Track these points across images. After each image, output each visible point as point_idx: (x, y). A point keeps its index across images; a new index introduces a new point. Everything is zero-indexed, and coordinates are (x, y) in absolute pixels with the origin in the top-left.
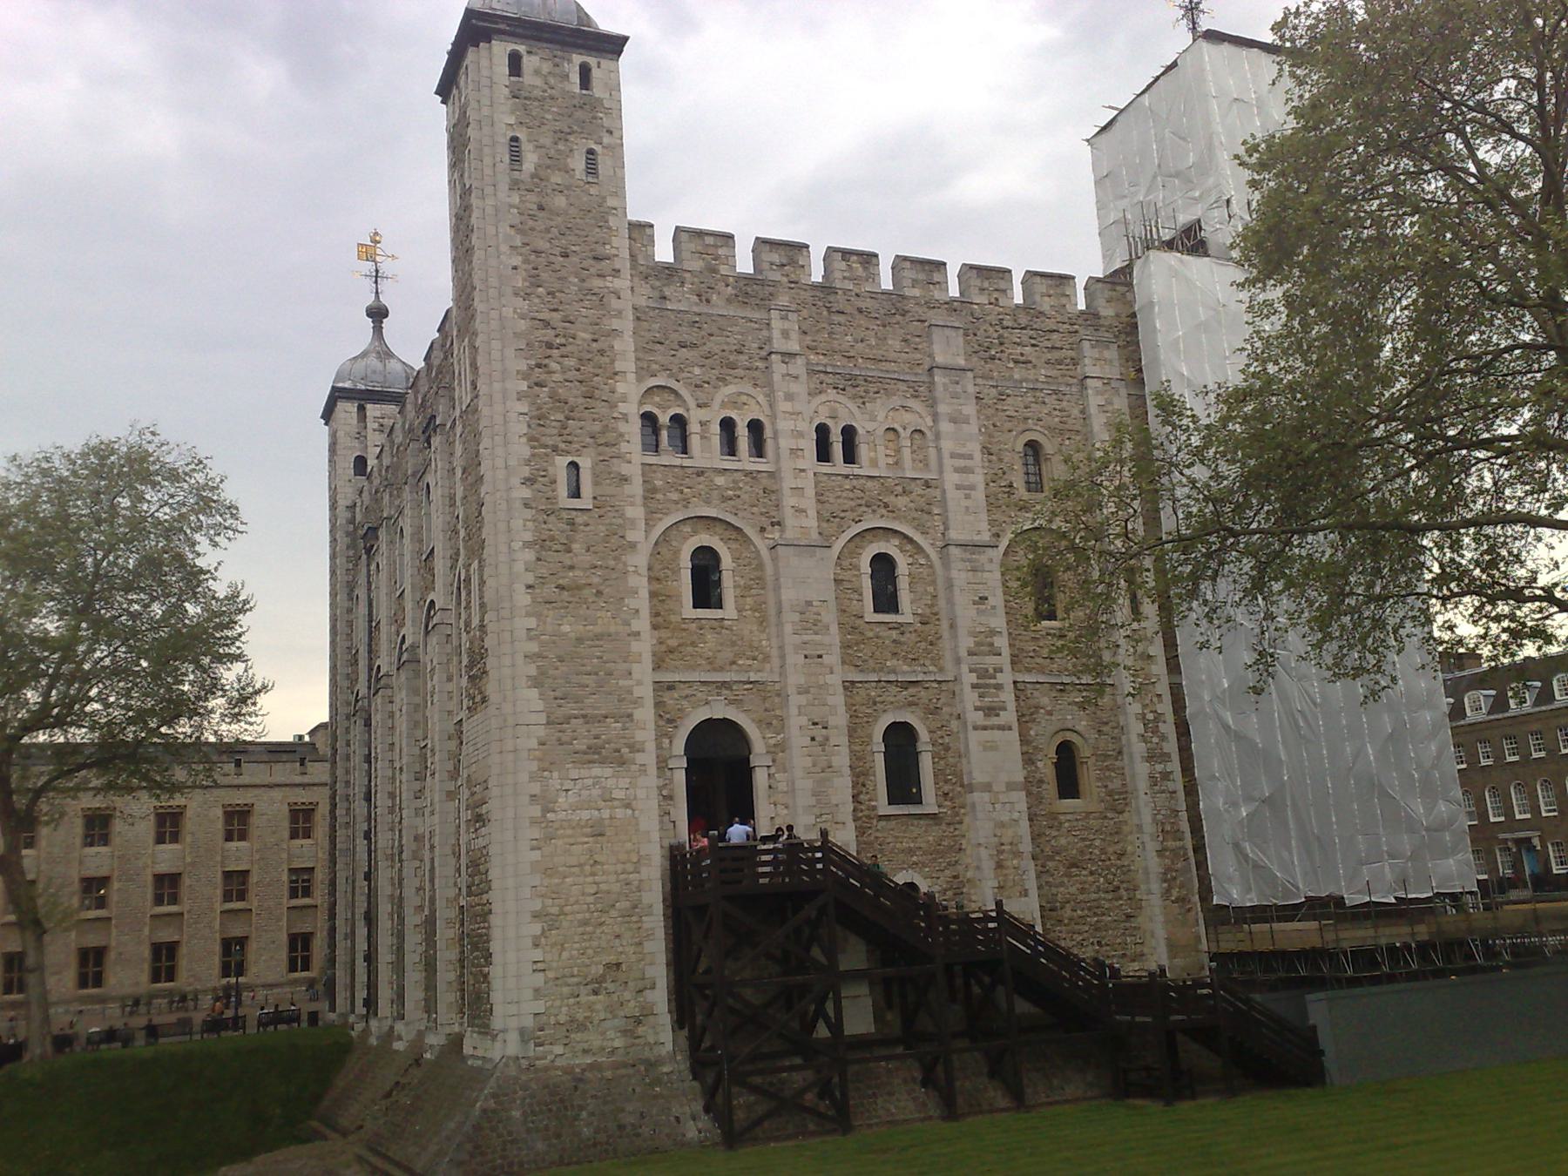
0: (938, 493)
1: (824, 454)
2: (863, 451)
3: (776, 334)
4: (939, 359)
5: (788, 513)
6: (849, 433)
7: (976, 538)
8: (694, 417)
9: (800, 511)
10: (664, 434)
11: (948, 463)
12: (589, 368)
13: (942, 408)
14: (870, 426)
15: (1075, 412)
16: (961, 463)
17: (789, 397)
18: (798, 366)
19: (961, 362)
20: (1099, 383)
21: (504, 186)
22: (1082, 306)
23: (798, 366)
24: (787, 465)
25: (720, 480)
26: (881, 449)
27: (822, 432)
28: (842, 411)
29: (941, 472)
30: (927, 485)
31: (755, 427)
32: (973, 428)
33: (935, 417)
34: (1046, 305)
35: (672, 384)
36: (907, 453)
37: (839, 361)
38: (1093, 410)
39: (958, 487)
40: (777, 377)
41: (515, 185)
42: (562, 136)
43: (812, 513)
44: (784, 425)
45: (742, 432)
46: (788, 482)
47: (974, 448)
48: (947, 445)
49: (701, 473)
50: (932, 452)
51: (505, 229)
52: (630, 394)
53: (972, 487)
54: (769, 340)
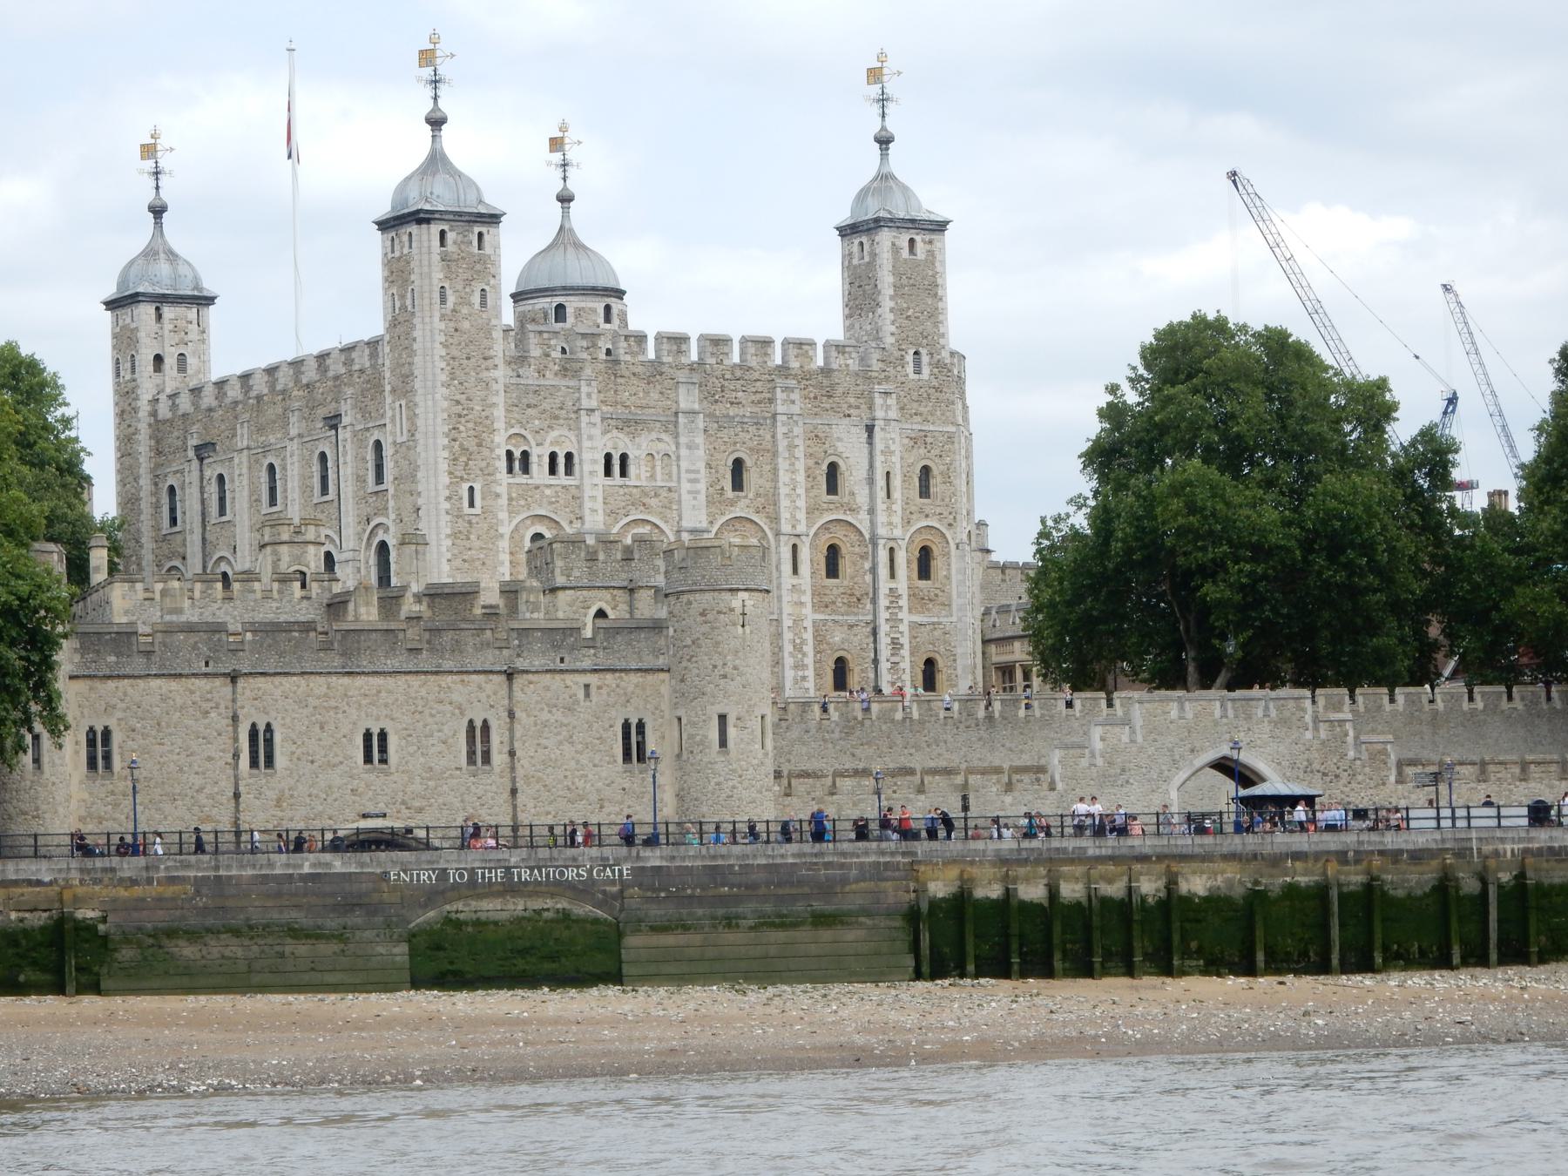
0: (675, 495)
1: (608, 472)
2: (632, 469)
3: (583, 396)
4: (683, 405)
5: (587, 512)
6: (624, 458)
7: (698, 526)
8: (535, 452)
9: (594, 511)
10: (517, 464)
11: (683, 475)
12: (480, 428)
13: (683, 440)
14: (637, 453)
15: (768, 437)
16: (693, 476)
17: (590, 438)
18: (596, 417)
19: (696, 407)
20: (784, 418)
21: (436, 319)
22: (778, 361)
23: (596, 417)
24: (587, 481)
25: (548, 492)
26: (643, 468)
27: (608, 457)
28: (619, 443)
29: (679, 481)
30: (670, 490)
31: (569, 456)
32: (701, 452)
33: (678, 445)
34: (753, 362)
35: (523, 432)
36: (658, 469)
37: (620, 409)
38: (779, 436)
39: (689, 492)
40: (583, 425)
41: (443, 317)
42: (468, 282)
43: (601, 512)
44: (586, 456)
45: (561, 461)
46: (588, 492)
47: (701, 465)
48: (684, 465)
49: (537, 487)
50: (675, 469)
51: (437, 345)
52: (500, 443)
53: (698, 492)
54: (579, 399)
